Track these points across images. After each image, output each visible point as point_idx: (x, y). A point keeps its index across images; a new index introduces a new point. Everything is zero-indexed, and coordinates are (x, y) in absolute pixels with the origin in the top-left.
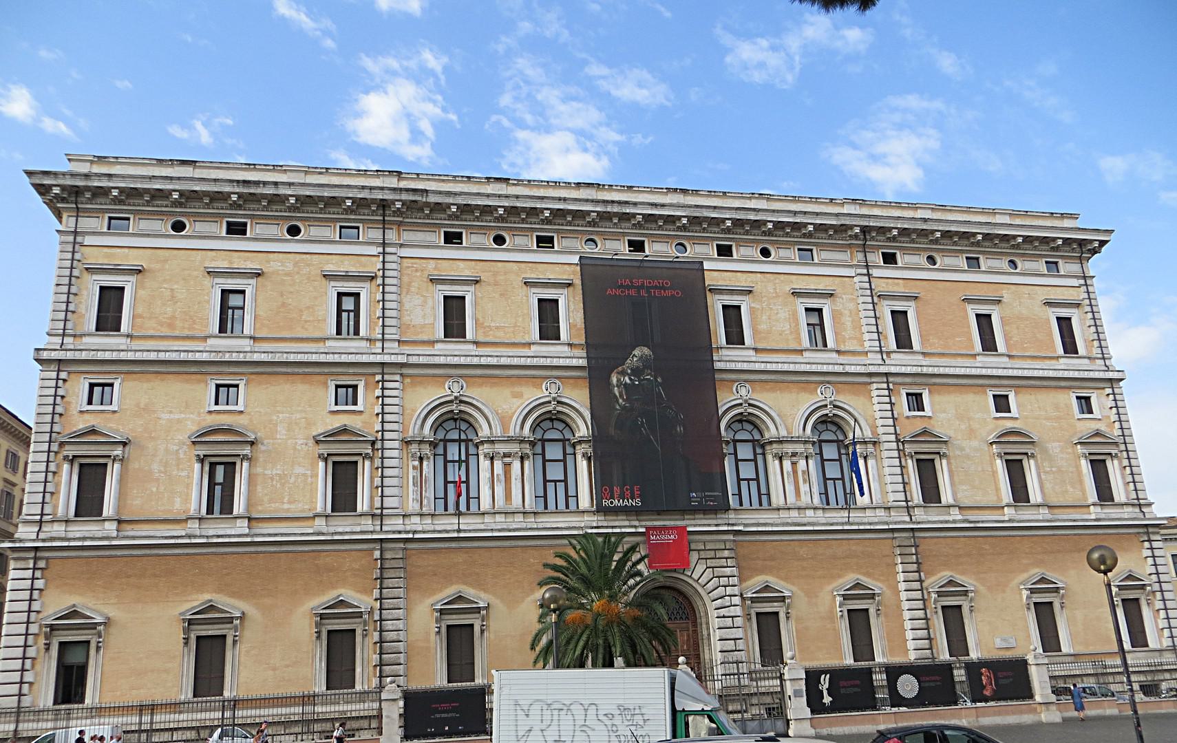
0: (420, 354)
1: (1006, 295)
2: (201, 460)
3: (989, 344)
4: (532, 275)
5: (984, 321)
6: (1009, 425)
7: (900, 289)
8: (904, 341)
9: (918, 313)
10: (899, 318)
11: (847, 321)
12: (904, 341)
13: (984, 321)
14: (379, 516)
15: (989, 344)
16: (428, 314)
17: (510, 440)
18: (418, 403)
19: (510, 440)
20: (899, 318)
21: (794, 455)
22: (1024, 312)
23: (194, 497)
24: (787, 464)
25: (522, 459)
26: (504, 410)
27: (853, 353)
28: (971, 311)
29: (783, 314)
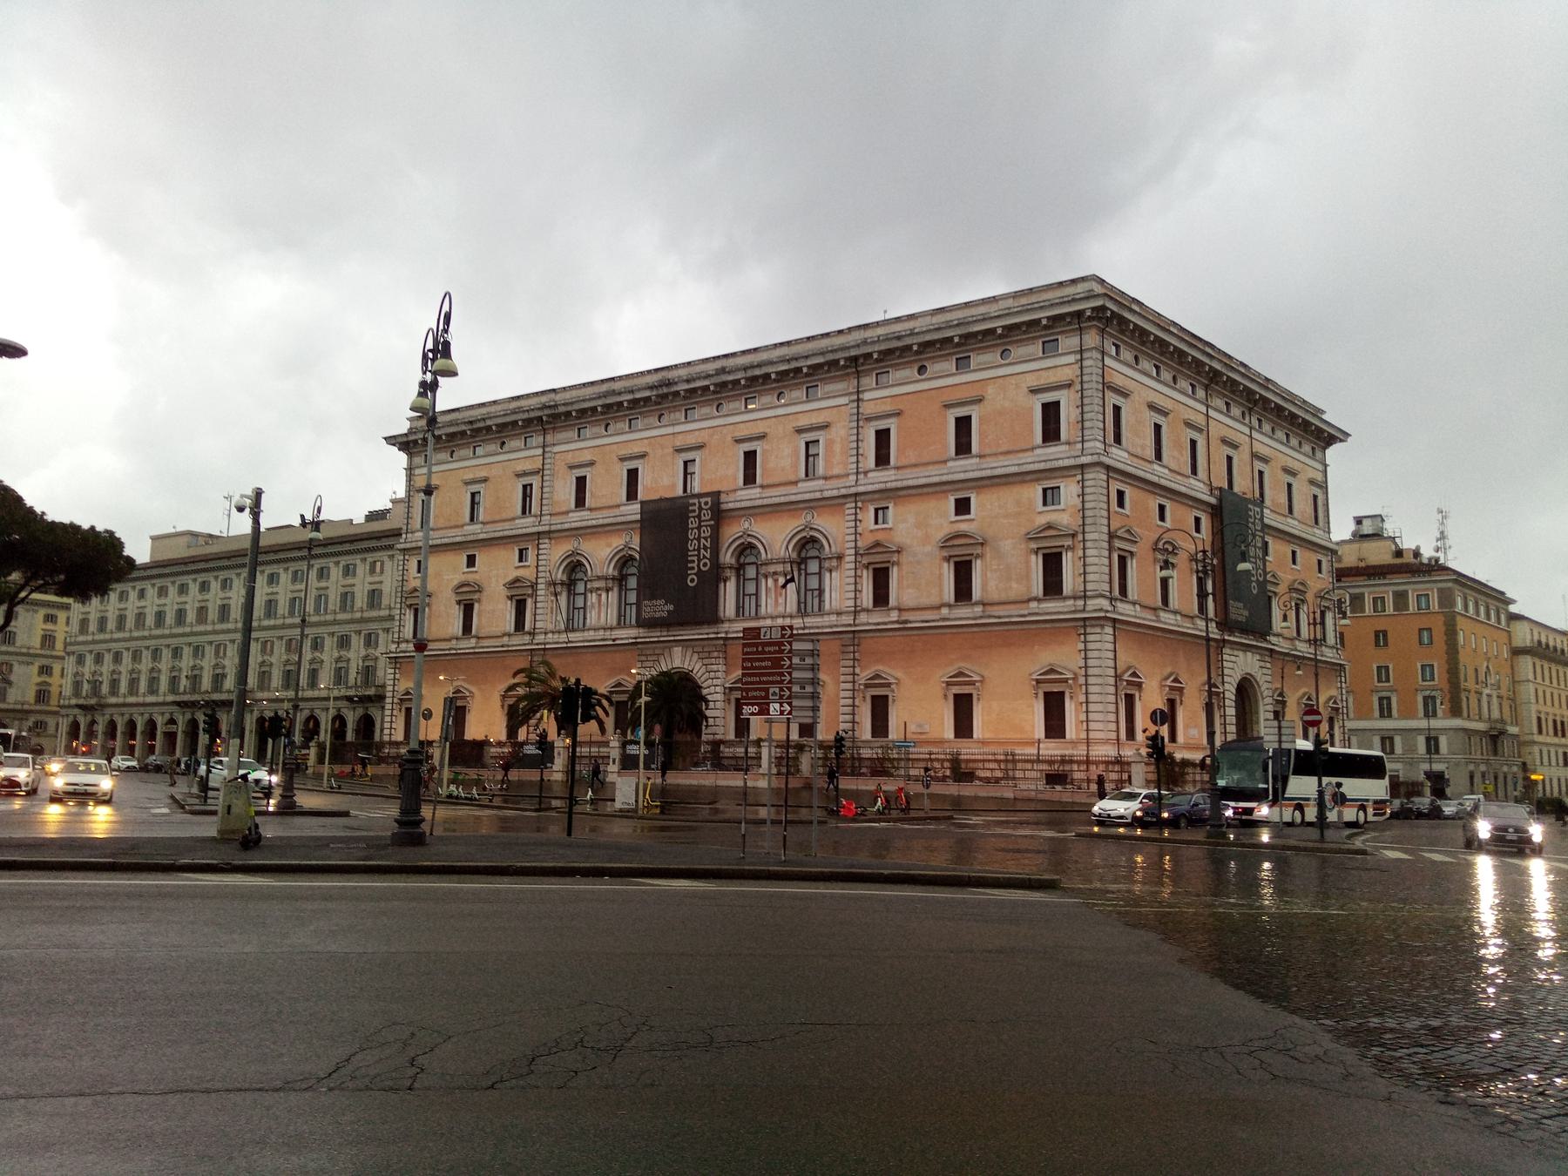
0: (558, 523)
1: (990, 391)
2: (459, 603)
3: (963, 447)
4: (624, 452)
5: (963, 425)
6: (964, 527)
7: (888, 407)
8: (882, 459)
9: (899, 427)
10: (883, 437)
11: (837, 448)
12: (882, 459)
13: (963, 425)
14: (532, 634)
15: (963, 447)
16: (564, 492)
17: (599, 578)
18: (554, 555)
19: (599, 578)
20: (883, 437)
21: (775, 573)
22: (1007, 404)
23: (457, 627)
24: (770, 581)
25: (607, 591)
26: (601, 554)
27: (838, 477)
28: (951, 416)
29: (787, 451)
